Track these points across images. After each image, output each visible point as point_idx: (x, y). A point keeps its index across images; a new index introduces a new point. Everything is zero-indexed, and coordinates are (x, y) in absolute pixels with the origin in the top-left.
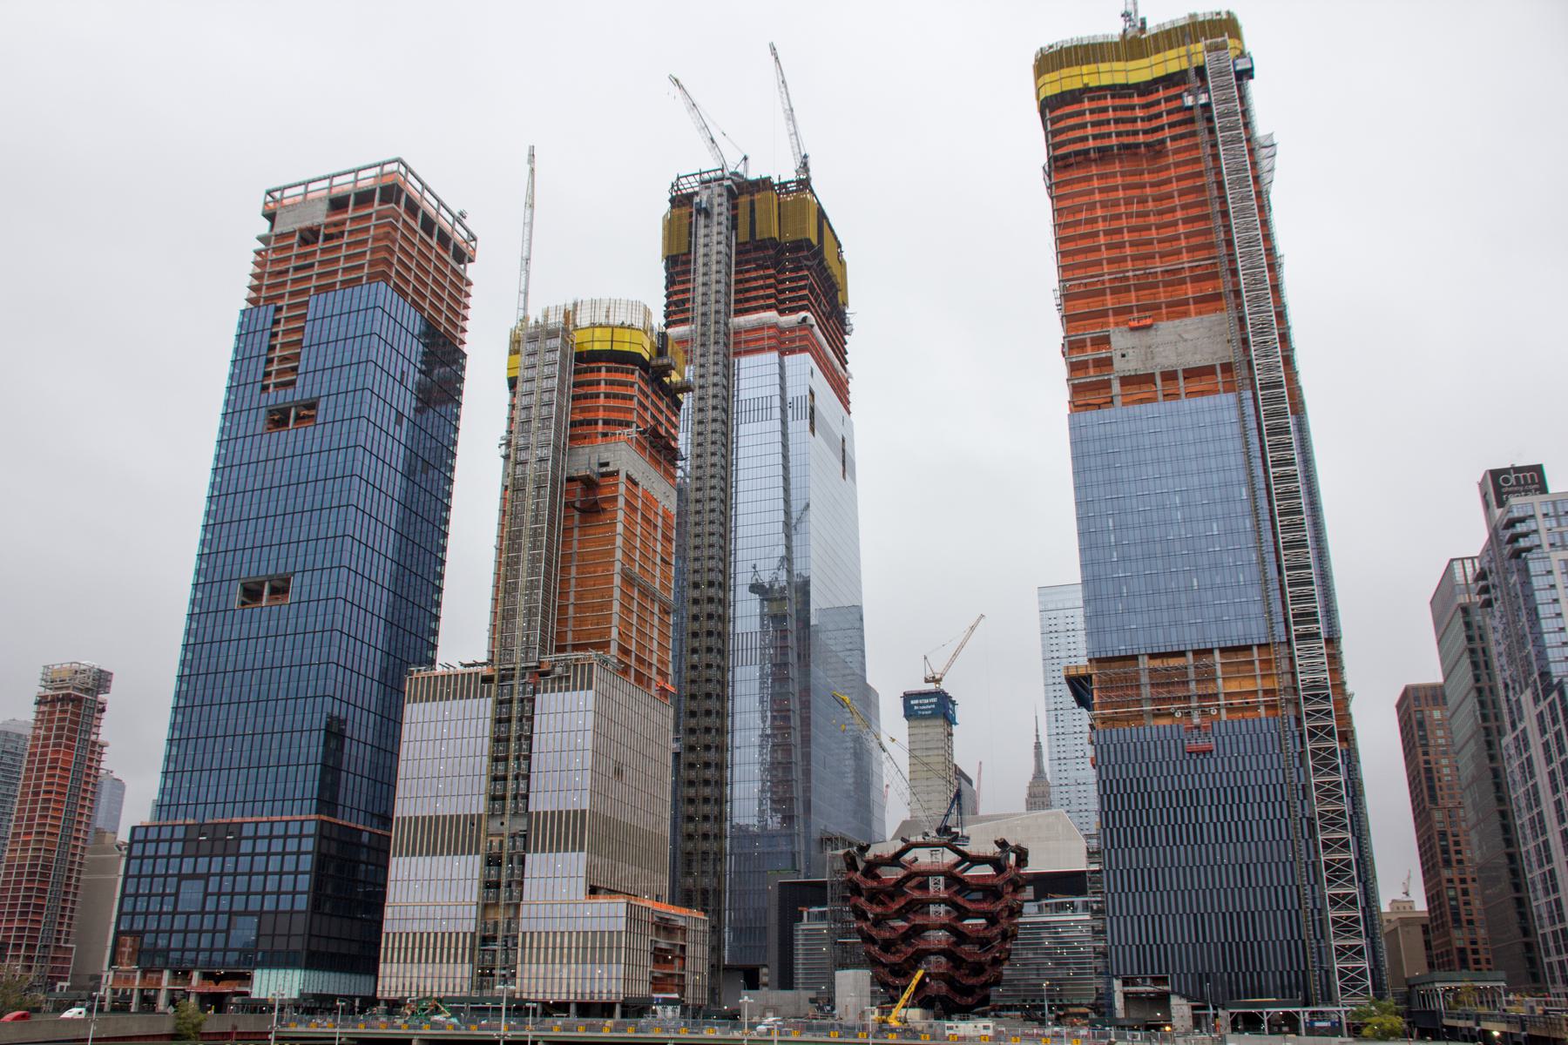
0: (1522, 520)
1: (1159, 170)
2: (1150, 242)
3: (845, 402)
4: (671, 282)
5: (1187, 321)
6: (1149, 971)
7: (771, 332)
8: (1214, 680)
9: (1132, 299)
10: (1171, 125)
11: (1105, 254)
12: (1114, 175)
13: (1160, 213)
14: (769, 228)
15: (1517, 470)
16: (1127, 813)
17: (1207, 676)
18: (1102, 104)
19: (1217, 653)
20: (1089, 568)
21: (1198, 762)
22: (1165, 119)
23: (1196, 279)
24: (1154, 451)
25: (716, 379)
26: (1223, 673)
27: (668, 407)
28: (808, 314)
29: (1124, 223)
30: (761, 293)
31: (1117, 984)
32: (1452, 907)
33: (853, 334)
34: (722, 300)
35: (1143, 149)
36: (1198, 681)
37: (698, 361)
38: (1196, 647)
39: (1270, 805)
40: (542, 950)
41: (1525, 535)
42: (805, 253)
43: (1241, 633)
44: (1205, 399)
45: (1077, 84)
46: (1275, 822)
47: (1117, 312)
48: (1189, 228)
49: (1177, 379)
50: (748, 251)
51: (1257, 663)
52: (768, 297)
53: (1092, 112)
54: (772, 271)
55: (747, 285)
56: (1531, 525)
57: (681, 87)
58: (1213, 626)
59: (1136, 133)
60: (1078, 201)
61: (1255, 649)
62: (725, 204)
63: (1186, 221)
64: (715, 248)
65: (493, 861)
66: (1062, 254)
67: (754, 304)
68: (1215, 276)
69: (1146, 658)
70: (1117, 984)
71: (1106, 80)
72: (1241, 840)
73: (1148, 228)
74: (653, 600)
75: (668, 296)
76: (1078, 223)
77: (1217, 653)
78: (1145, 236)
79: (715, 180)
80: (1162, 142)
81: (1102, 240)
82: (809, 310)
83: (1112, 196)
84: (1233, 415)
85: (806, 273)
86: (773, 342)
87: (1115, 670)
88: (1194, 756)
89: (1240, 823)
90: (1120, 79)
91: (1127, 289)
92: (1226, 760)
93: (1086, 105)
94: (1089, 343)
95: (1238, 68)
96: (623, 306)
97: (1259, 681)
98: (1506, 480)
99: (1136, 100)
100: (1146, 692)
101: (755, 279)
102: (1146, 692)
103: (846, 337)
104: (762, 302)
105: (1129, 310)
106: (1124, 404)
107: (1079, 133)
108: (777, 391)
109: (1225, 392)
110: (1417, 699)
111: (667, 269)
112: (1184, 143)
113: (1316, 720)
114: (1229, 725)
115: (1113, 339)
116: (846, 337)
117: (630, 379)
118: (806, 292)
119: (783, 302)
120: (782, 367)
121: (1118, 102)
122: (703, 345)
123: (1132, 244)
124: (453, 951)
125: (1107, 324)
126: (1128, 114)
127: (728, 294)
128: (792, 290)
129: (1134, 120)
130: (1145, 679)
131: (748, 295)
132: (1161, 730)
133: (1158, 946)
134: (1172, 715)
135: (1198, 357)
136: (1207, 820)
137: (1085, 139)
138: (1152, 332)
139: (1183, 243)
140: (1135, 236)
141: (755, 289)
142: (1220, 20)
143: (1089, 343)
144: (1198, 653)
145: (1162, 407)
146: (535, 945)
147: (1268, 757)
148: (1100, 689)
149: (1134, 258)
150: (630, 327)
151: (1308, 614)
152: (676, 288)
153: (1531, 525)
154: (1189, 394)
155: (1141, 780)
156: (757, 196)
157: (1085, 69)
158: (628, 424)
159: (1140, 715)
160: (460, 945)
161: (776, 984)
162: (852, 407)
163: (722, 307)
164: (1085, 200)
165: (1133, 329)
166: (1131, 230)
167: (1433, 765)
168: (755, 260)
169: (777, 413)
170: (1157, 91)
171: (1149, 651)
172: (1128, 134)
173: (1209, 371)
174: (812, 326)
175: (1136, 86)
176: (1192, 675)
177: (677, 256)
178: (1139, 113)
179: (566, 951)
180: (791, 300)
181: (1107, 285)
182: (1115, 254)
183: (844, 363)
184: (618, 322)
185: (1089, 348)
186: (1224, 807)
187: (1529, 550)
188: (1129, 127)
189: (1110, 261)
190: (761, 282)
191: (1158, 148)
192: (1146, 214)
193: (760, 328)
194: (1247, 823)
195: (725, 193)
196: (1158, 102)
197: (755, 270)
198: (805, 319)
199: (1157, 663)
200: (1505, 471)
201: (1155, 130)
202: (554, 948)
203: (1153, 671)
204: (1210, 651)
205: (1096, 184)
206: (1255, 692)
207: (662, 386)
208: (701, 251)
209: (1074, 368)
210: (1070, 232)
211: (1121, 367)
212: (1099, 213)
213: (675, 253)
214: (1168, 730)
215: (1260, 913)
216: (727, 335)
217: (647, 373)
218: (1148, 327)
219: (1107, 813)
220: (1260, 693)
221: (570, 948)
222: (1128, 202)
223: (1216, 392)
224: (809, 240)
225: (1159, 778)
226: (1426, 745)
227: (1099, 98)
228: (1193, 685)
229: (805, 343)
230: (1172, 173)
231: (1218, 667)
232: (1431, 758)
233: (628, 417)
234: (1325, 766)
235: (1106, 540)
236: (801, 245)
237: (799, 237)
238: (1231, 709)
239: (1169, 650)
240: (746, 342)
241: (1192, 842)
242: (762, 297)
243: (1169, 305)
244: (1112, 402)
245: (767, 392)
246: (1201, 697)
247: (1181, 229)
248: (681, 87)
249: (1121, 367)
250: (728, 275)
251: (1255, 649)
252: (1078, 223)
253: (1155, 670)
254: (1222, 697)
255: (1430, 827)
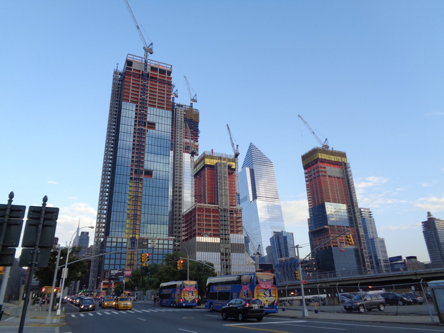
19: (345, 227)
65: (222, 254)
77: (345, 227)
100: (337, 232)
115: (326, 168)
144: (343, 227)
211: (328, 173)
249: (328, 173)
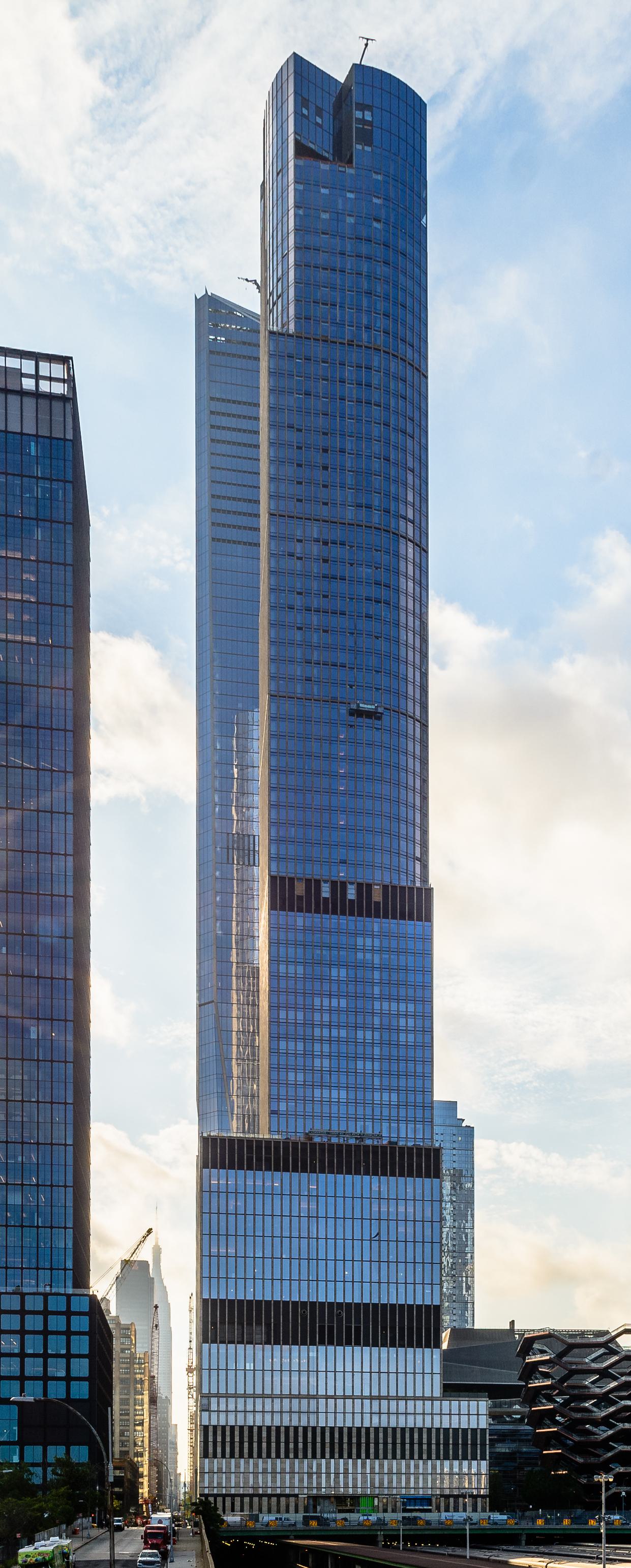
40: (399, 1446)
124: (291, 1446)
146: (390, 1440)
160: (300, 1439)
179: (425, 1447)
202: (412, 1444)
221: (429, 1444)
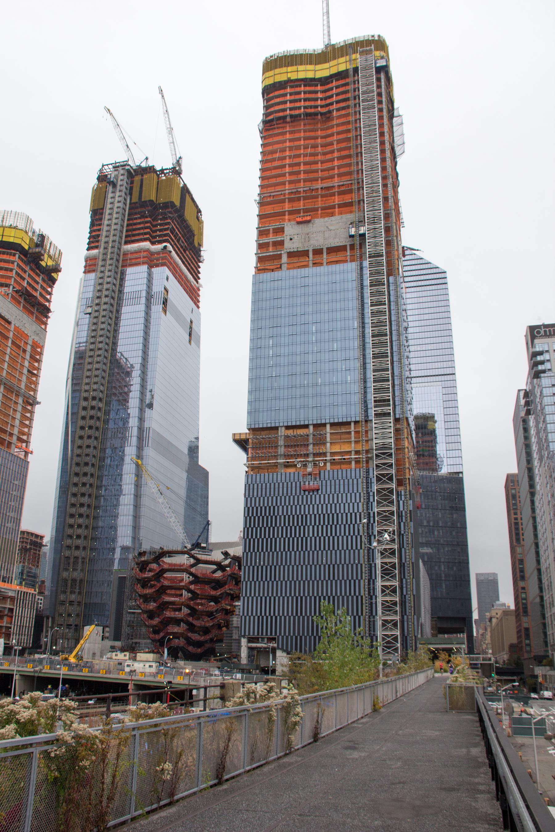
0: (541, 353)
1: (327, 129)
2: (316, 171)
3: (196, 302)
4: (92, 224)
5: (333, 218)
6: (264, 634)
7: (145, 254)
8: (325, 444)
9: (301, 205)
10: (338, 102)
11: (288, 178)
12: (299, 131)
13: (324, 154)
14: (150, 194)
15: (545, 326)
16: (265, 528)
17: (320, 441)
18: (298, 89)
19: (328, 426)
20: (254, 371)
21: (309, 496)
22: (334, 99)
23: (341, 193)
24: (303, 298)
25: (109, 280)
26: (331, 439)
27: (43, 280)
28: (168, 245)
29: (302, 159)
30: (142, 231)
31: (244, 641)
32: (523, 604)
33: (204, 262)
34: (118, 235)
35: (319, 117)
36: (314, 444)
37: (100, 269)
38: (315, 422)
39: (352, 526)
41: (542, 363)
42: (170, 210)
43: (344, 414)
44: (338, 266)
45: (284, 78)
46: (354, 537)
47: (291, 213)
48: (341, 162)
49: (322, 253)
50: (137, 208)
51: (353, 433)
52: (146, 234)
53: (291, 94)
54: (149, 219)
55: (134, 227)
56: (546, 356)
57: (111, 114)
58: (327, 409)
59: (316, 107)
60: (275, 147)
61: (352, 424)
62: (126, 179)
63: (339, 158)
64: (117, 205)
66: (262, 178)
67: (137, 238)
68: (350, 191)
69: (283, 428)
70: (244, 641)
71: (301, 76)
72: (331, 549)
73: (316, 163)
74: (17, 395)
75: (90, 233)
76: (273, 160)
77: (328, 426)
78: (314, 167)
79: (122, 166)
80: (330, 112)
81: (287, 170)
82: (169, 242)
83: (297, 143)
84: (354, 275)
85: (169, 221)
86: (146, 260)
87: (264, 435)
88: (307, 493)
89: (331, 538)
90: (310, 75)
91: (299, 199)
92: (327, 496)
93: (288, 90)
94: (271, 231)
95: (378, 65)
96: (13, 215)
97: (353, 445)
98: (538, 332)
99: (319, 88)
100: (281, 450)
101: (140, 223)
102: (281, 450)
103: (200, 264)
104: (142, 237)
105: (298, 212)
106: (288, 269)
107: (282, 107)
108: (145, 287)
109: (351, 261)
110: (512, 481)
111: (91, 217)
112: (343, 112)
113: (383, 469)
114: (331, 473)
115: (285, 229)
116: (200, 264)
117: (12, 258)
118: (169, 232)
119: (155, 237)
120: (150, 275)
121: (308, 89)
122: (104, 260)
123: (305, 172)
125: (284, 220)
126: (313, 96)
127: (121, 232)
128: (160, 230)
129: (316, 100)
130: (281, 442)
131: (134, 233)
132: (288, 475)
133: (272, 617)
134: (295, 466)
135: (337, 240)
136: (311, 535)
137: (284, 110)
138: (310, 225)
139: (336, 172)
140: (308, 168)
141: (139, 229)
142: (373, 40)
143: (271, 231)
144: (316, 426)
145: (311, 271)
147: (349, 495)
148: (253, 448)
149: (305, 181)
150: (16, 228)
151: (384, 401)
152: (95, 228)
153: (546, 356)
154: (329, 263)
155: (272, 508)
156: (145, 176)
157: (290, 69)
158: (7, 286)
159: (276, 465)
161: (112, 637)
162: (200, 305)
163: (117, 238)
164: (280, 146)
165: (299, 223)
166: (305, 164)
167: (519, 520)
168: (140, 213)
169: (143, 300)
170: (332, 82)
171: (286, 424)
172: (311, 107)
173: (342, 248)
174: (171, 252)
175: (320, 80)
176: (311, 441)
177: (97, 210)
178: (320, 95)
180: (160, 236)
181: (287, 197)
182: (294, 178)
183: (197, 279)
184: (7, 224)
185: (271, 234)
186: (322, 527)
187: (544, 372)
188: (312, 103)
189: (290, 182)
190: (142, 226)
191: (328, 115)
192: (316, 155)
193: (139, 251)
194: (336, 538)
195: (126, 174)
196: (332, 89)
197: (140, 218)
198: (165, 247)
199: (290, 432)
200: (538, 327)
201: (327, 105)
203: (287, 437)
204: (324, 425)
205: (288, 136)
206: (349, 453)
207: (39, 267)
208: (109, 206)
209: (261, 246)
210: (269, 165)
212: (288, 153)
213: (96, 208)
214: (292, 475)
215: (338, 597)
216: (119, 255)
217: (26, 256)
218: (309, 222)
219: (248, 529)
220: (353, 453)
222: (306, 147)
223: (346, 261)
224: (172, 203)
225: (283, 507)
226: (516, 509)
227: (297, 86)
228: (311, 447)
229: (164, 261)
230: (335, 130)
231: (328, 436)
232: (519, 516)
233: (8, 282)
234: (385, 500)
235: (267, 353)
236: (169, 205)
237: (167, 201)
238: (333, 462)
239: (298, 423)
240: (130, 259)
241: (300, 549)
242: (142, 234)
243: (323, 209)
244: (281, 268)
245: (139, 288)
246: (315, 455)
247: (336, 163)
248: (111, 114)
249: (289, 246)
250: (123, 220)
251: (352, 424)
252: (273, 160)
253: (288, 437)
254: (328, 454)
255: (515, 558)
